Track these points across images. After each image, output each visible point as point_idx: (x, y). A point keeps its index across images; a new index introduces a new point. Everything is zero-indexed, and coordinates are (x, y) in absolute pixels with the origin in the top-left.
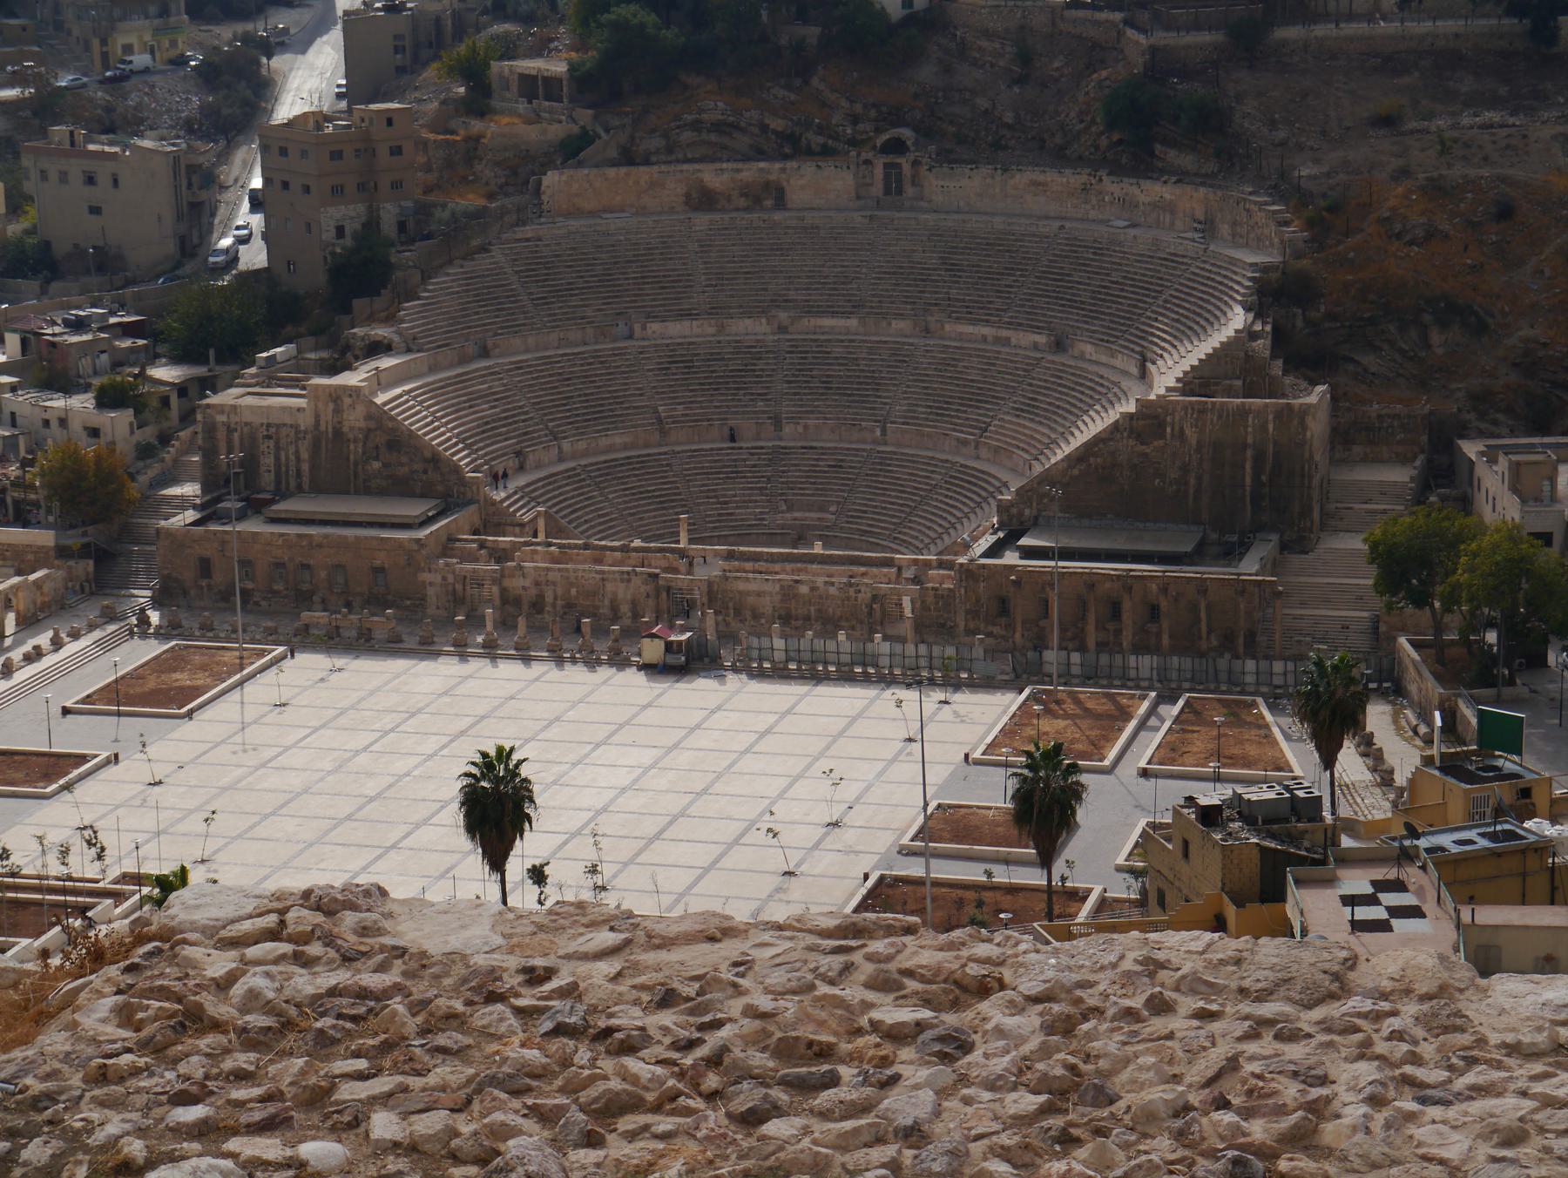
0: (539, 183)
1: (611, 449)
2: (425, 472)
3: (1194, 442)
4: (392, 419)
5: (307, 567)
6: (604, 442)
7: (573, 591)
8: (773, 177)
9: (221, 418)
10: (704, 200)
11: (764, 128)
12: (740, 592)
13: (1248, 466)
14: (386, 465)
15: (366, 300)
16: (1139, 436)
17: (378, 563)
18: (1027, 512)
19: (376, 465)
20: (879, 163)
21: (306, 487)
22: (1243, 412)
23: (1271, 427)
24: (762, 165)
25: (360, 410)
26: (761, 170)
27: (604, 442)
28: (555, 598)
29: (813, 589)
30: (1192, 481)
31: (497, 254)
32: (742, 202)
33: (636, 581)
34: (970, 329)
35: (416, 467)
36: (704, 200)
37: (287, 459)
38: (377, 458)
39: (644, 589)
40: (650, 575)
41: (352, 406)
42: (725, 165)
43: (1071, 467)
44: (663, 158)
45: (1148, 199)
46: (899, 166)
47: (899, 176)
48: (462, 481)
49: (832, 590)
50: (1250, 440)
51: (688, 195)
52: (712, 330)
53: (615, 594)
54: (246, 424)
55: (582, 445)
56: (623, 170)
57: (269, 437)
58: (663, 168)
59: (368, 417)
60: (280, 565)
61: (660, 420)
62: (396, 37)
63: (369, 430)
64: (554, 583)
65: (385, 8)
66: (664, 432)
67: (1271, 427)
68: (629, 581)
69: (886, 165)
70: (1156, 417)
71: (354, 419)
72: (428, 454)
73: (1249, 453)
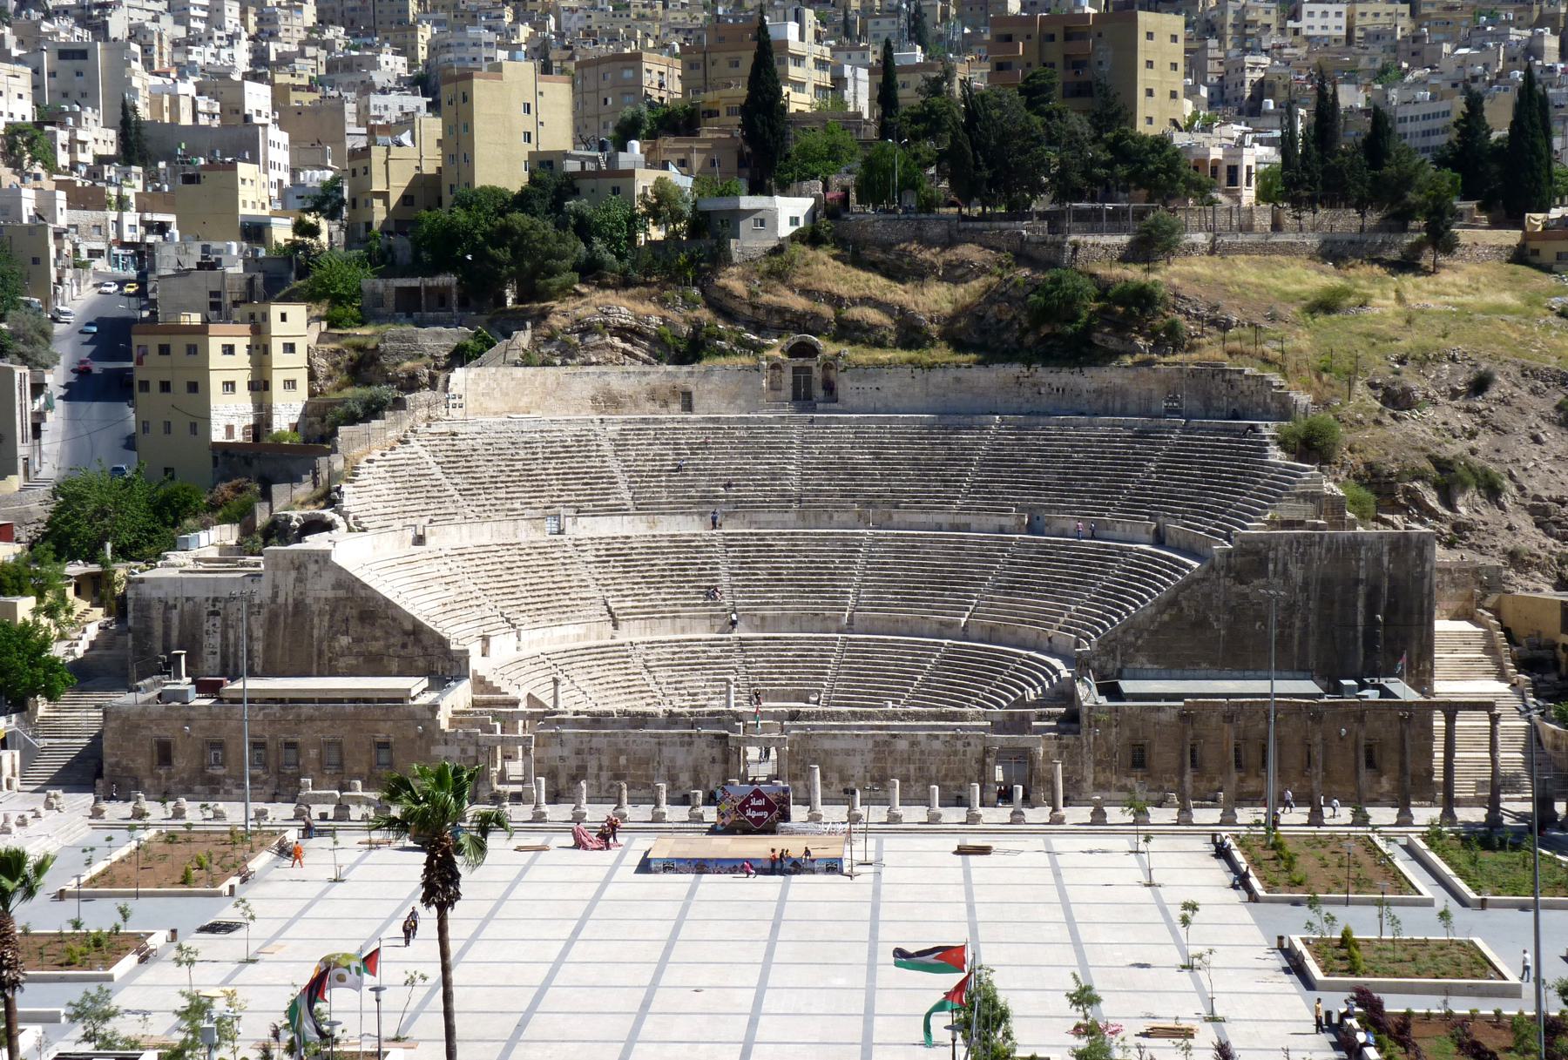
0: (447, 381)
1: (564, 638)
2: (404, 646)
3: (1299, 579)
4: (365, 586)
5: (291, 745)
7: (623, 760)
8: (680, 382)
9: (155, 594)
10: (610, 401)
12: (826, 752)
13: (1360, 604)
14: (358, 640)
15: (285, 487)
17: (381, 737)
18: (1110, 666)
19: (345, 640)
21: (258, 669)
22: (1355, 544)
23: (1386, 559)
24: (671, 368)
25: (328, 578)
26: (668, 373)
27: (558, 631)
28: (600, 768)
29: (913, 744)
30: (1298, 624)
31: (415, 445)
32: (649, 406)
33: (700, 745)
34: (922, 518)
35: (392, 640)
36: (610, 401)
37: (237, 639)
38: (346, 633)
39: (708, 752)
40: (717, 736)
41: (318, 574)
42: (631, 368)
43: (1161, 612)
45: (1094, 385)
46: (809, 370)
47: (808, 381)
49: (937, 745)
50: (1362, 575)
51: (594, 399)
53: (672, 760)
54: (188, 599)
56: (530, 370)
57: (215, 613)
59: (338, 585)
62: (213, 294)
63: (337, 600)
64: (598, 751)
65: (200, 266)
66: (615, 626)
67: (1386, 559)
68: (691, 744)
69: (795, 370)
70: (1258, 553)
71: (320, 589)
72: (408, 626)
73: (1361, 589)
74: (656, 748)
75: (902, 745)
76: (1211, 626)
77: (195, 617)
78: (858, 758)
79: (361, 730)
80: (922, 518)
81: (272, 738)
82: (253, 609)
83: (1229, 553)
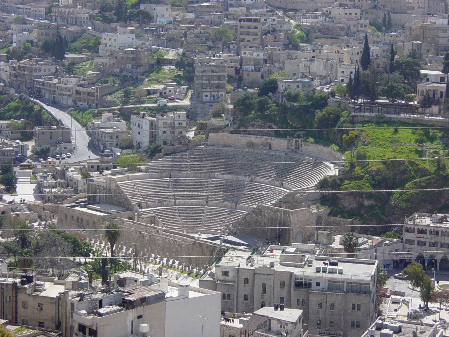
5: (82, 220)
6: (189, 203)
8: (268, 141)
16: (256, 214)
20: (294, 140)
24: (266, 137)
32: (261, 147)
43: (243, 220)
44: (244, 133)
48: (131, 205)
51: (248, 143)
52: (235, 179)
55: (182, 202)
56: (231, 135)
57: (98, 188)
58: (242, 135)
59: (116, 186)
60: (78, 218)
61: (207, 199)
69: (296, 141)
70: (260, 209)
71: (113, 186)
75: (167, 240)
77: (96, 188)
80: (288, 186)
82: (104, 189)
83: (255, 208)
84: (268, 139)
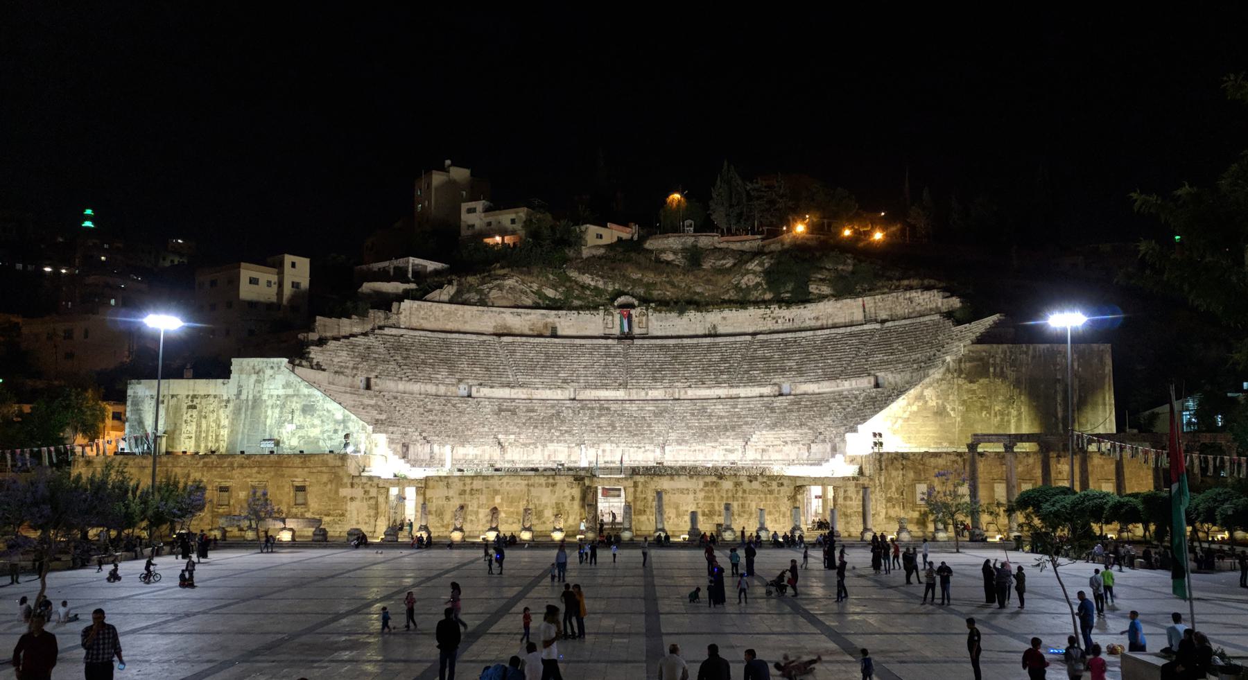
5: (224, 489)
8: (549, 320)
11: (538, 293)
35: (326, 428)
37: (208, 426)
38: (291, 422)
56: (454, 307)
57: (194, 407)
63: (287, 396)
68: (554, 485)
70: (981, 359)
73: (1059, 387)
74: (525, 489)
76: (949, 415)
78: (691, 496)
79: (283, 476)
81: (209, 482)
84: (547, 317)
